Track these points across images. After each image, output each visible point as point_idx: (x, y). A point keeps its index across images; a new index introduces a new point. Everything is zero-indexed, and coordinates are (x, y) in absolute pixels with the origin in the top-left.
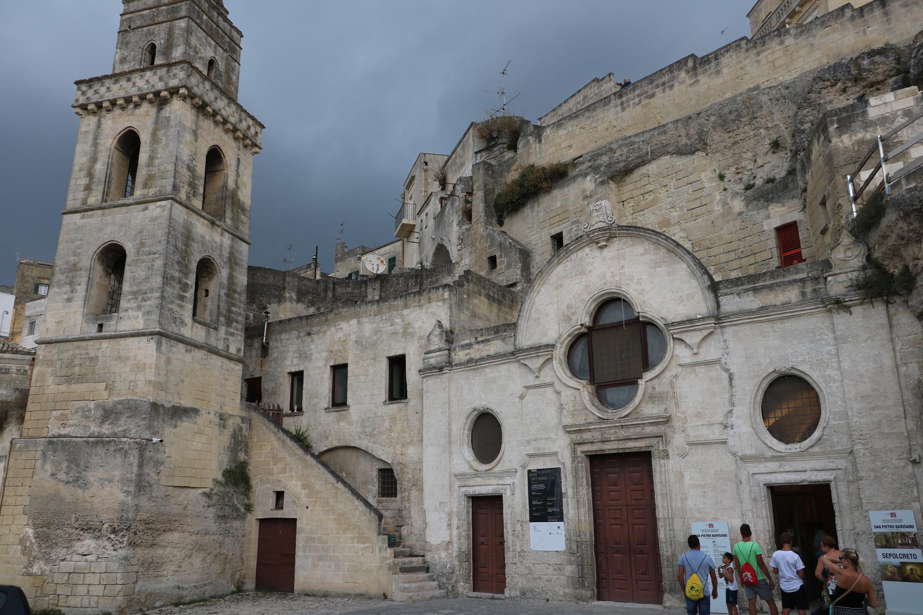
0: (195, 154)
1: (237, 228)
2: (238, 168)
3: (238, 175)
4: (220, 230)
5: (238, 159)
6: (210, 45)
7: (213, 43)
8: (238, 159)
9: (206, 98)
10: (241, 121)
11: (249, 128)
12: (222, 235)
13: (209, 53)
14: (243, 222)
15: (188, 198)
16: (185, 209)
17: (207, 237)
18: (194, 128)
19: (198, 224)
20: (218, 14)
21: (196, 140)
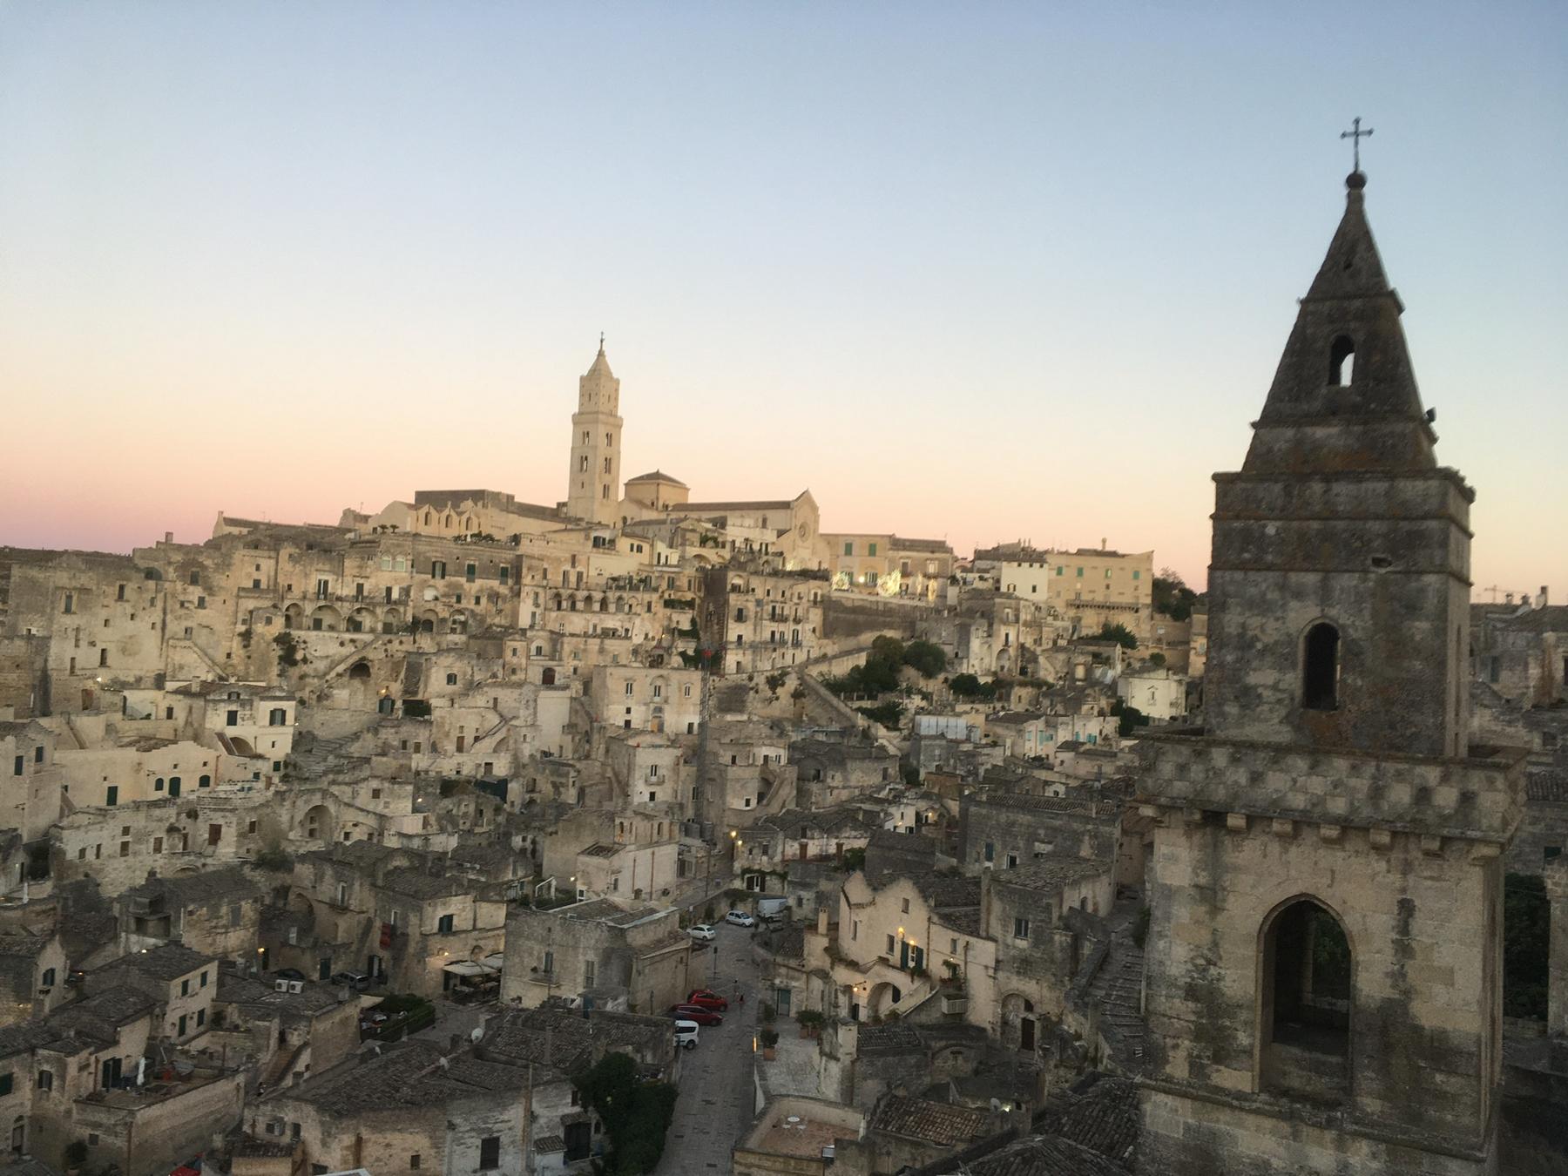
0: (1215, 945)
1: (1416, 1118)
2: (1404, 929)
3: (1404, 948)
4: (1330, 1135)
5: (1406, 908)
6: (1299, 595)
7: (1311, 579)
8: (1406, 908)
9: (1220, 794)
10: (1377, 793)
11: (1423, 795)
12: (1340, 1145)
13: (1301, 616)
14: (1441, 1096)
15: (1196, 1066)
16: (1188, 1103)
17: (1275, 1163)
18: (1203, 880)
19: (1239, 1132)
20: (1328, 479)
21: (1215, 909)
